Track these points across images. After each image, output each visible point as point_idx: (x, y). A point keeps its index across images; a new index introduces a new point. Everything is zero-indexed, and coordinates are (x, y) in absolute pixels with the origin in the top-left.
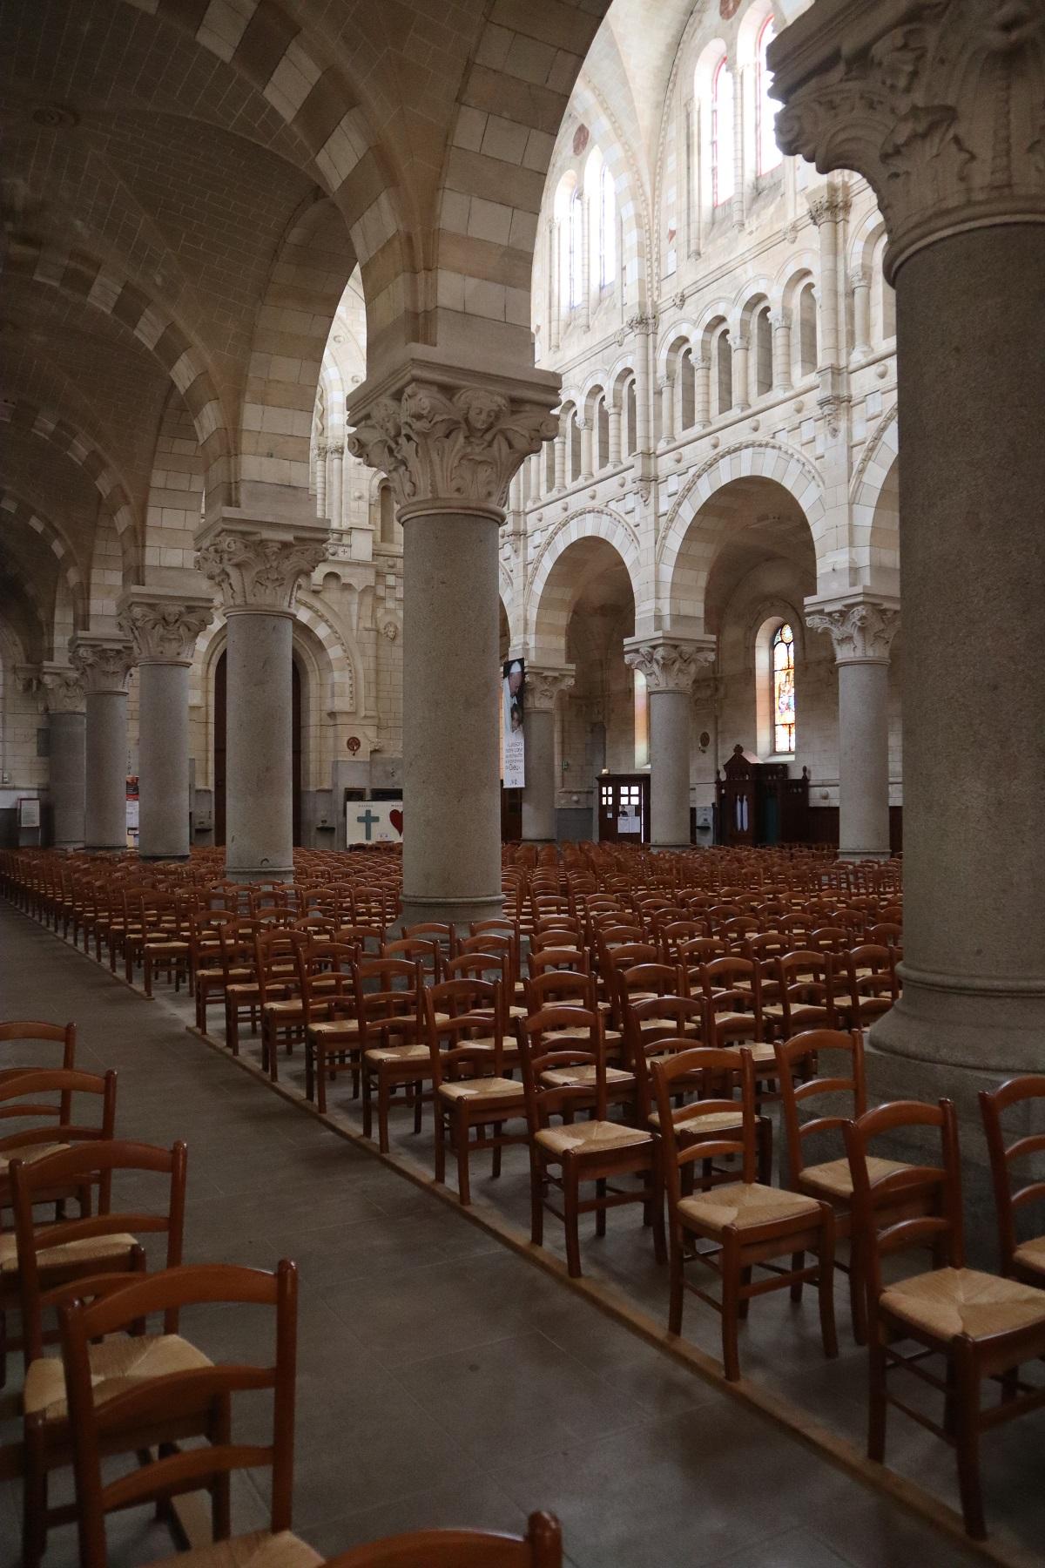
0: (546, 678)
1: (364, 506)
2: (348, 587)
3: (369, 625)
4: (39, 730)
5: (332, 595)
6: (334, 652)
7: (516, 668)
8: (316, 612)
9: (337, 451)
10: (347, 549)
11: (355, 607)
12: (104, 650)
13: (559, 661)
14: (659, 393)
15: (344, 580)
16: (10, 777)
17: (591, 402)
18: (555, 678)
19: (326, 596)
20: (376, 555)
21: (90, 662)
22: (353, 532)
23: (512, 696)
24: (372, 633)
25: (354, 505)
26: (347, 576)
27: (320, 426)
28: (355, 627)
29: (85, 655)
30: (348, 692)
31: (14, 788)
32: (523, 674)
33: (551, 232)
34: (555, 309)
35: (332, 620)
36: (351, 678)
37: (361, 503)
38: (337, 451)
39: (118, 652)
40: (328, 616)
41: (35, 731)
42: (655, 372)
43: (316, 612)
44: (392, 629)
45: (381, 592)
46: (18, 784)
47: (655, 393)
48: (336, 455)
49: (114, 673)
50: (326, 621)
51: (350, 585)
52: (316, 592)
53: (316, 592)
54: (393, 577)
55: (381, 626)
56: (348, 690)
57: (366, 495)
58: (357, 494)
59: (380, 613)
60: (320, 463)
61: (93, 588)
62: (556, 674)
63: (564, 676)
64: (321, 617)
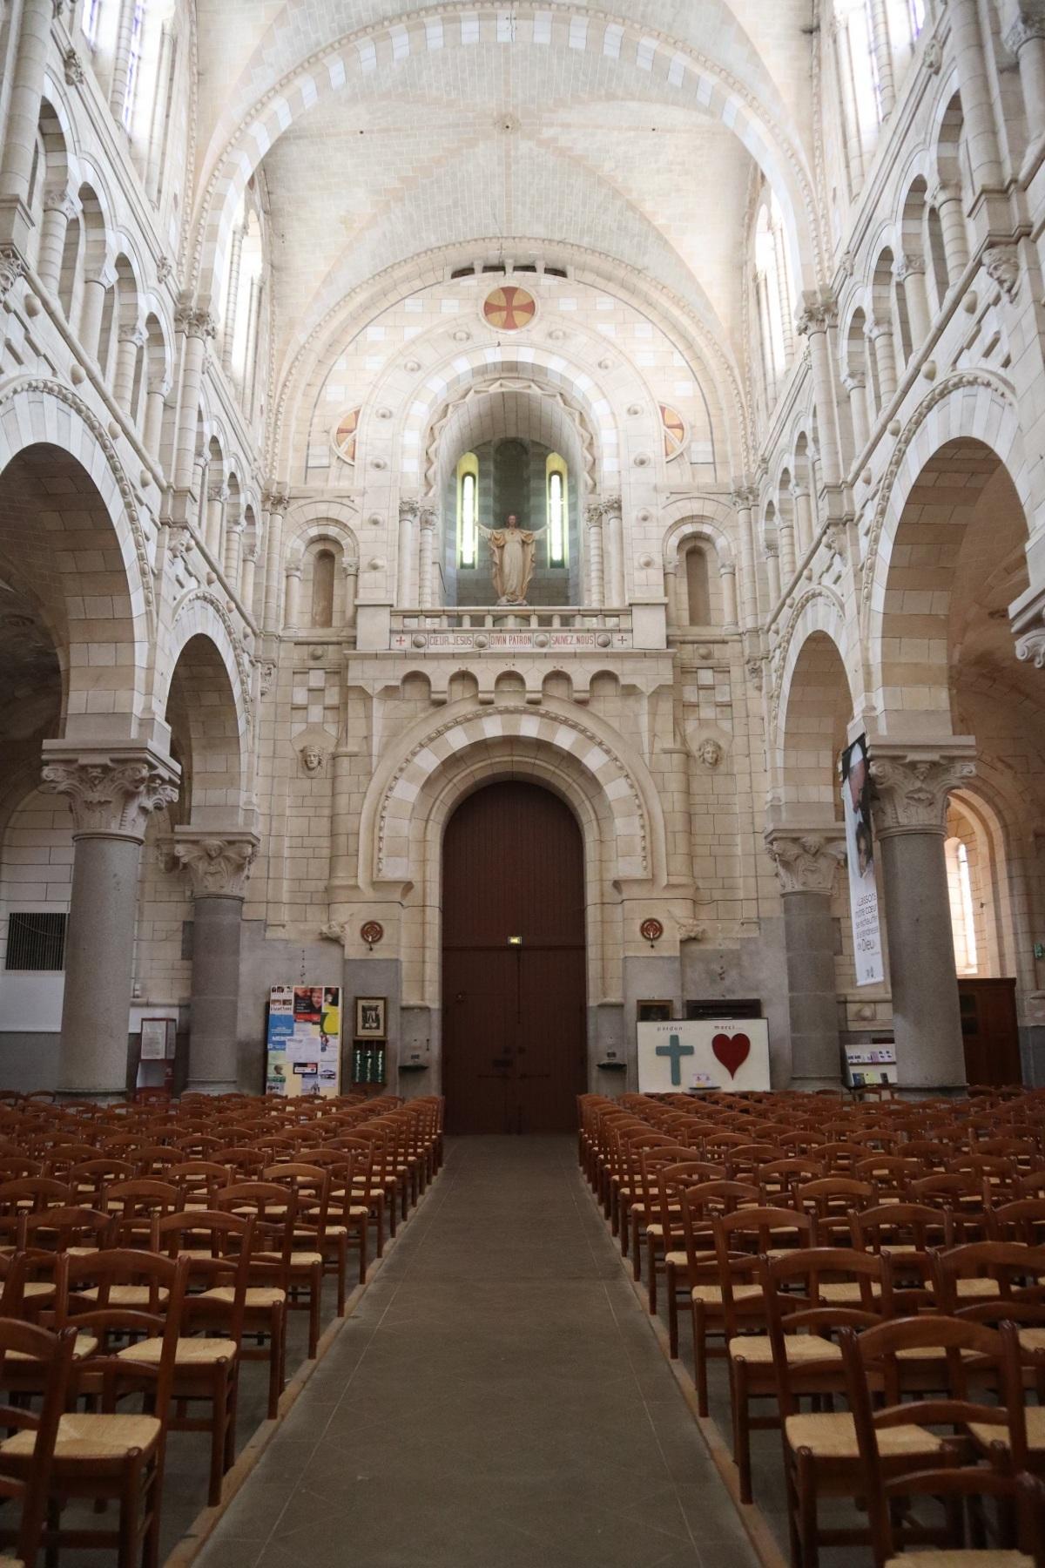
0: (913, 765)
1: (656, 576)
2: (631, 691)
3: (669, 744)
4: (185, 923)
5: (608, 704)
6: (615, 789)
7: (857, 757)
8: (583, 731)
9: (611, 507)
10: (625, 636)
11: (644, 720)
12: (84, 768)
13: (941, 733)
14: (1011, 69)
15: (624, 681)
16: (143, 989)
17: (913, 226)
18: (934, 764)
19: (597, 707)
20: (669, 643)
21: (62, 787)
22: (635, 609)
23: (856, 811)
24: (675, 756)
25: (640, 576)
26: (628, 673)
27: (590, 482)
28: (646, 750)
29: (52, 776)
30: (639, 849)
31: (148, 1005)
32: (866, 762)
33: (835, 41)
34: (853, 143)
35: (608, 743)
36: (643, 827)
37: (650, 571)
38: (611, 507)
39: (105, 769)
40: (600, 734)
41: (178, 925)
42: (997, 33)
43: (583, 731)
44: (710, 749)
45: (690, 695)
46: (154, 999)
47: (1001, 71)
48: (612, 514)
49: (100, 804)
50: (600, 744)
51: (634, 686)
52: (582, 703)
53: (582, 703)
54: (710, 672)
55: (694, 747)
56: (639, 844)
57: (658, 560)
58: (643, 560)
59: (691, 726)
60: (594, 530)
61: (73, 673)
62: (934, 756)
63: (952, 759)
64: (592, 738)
